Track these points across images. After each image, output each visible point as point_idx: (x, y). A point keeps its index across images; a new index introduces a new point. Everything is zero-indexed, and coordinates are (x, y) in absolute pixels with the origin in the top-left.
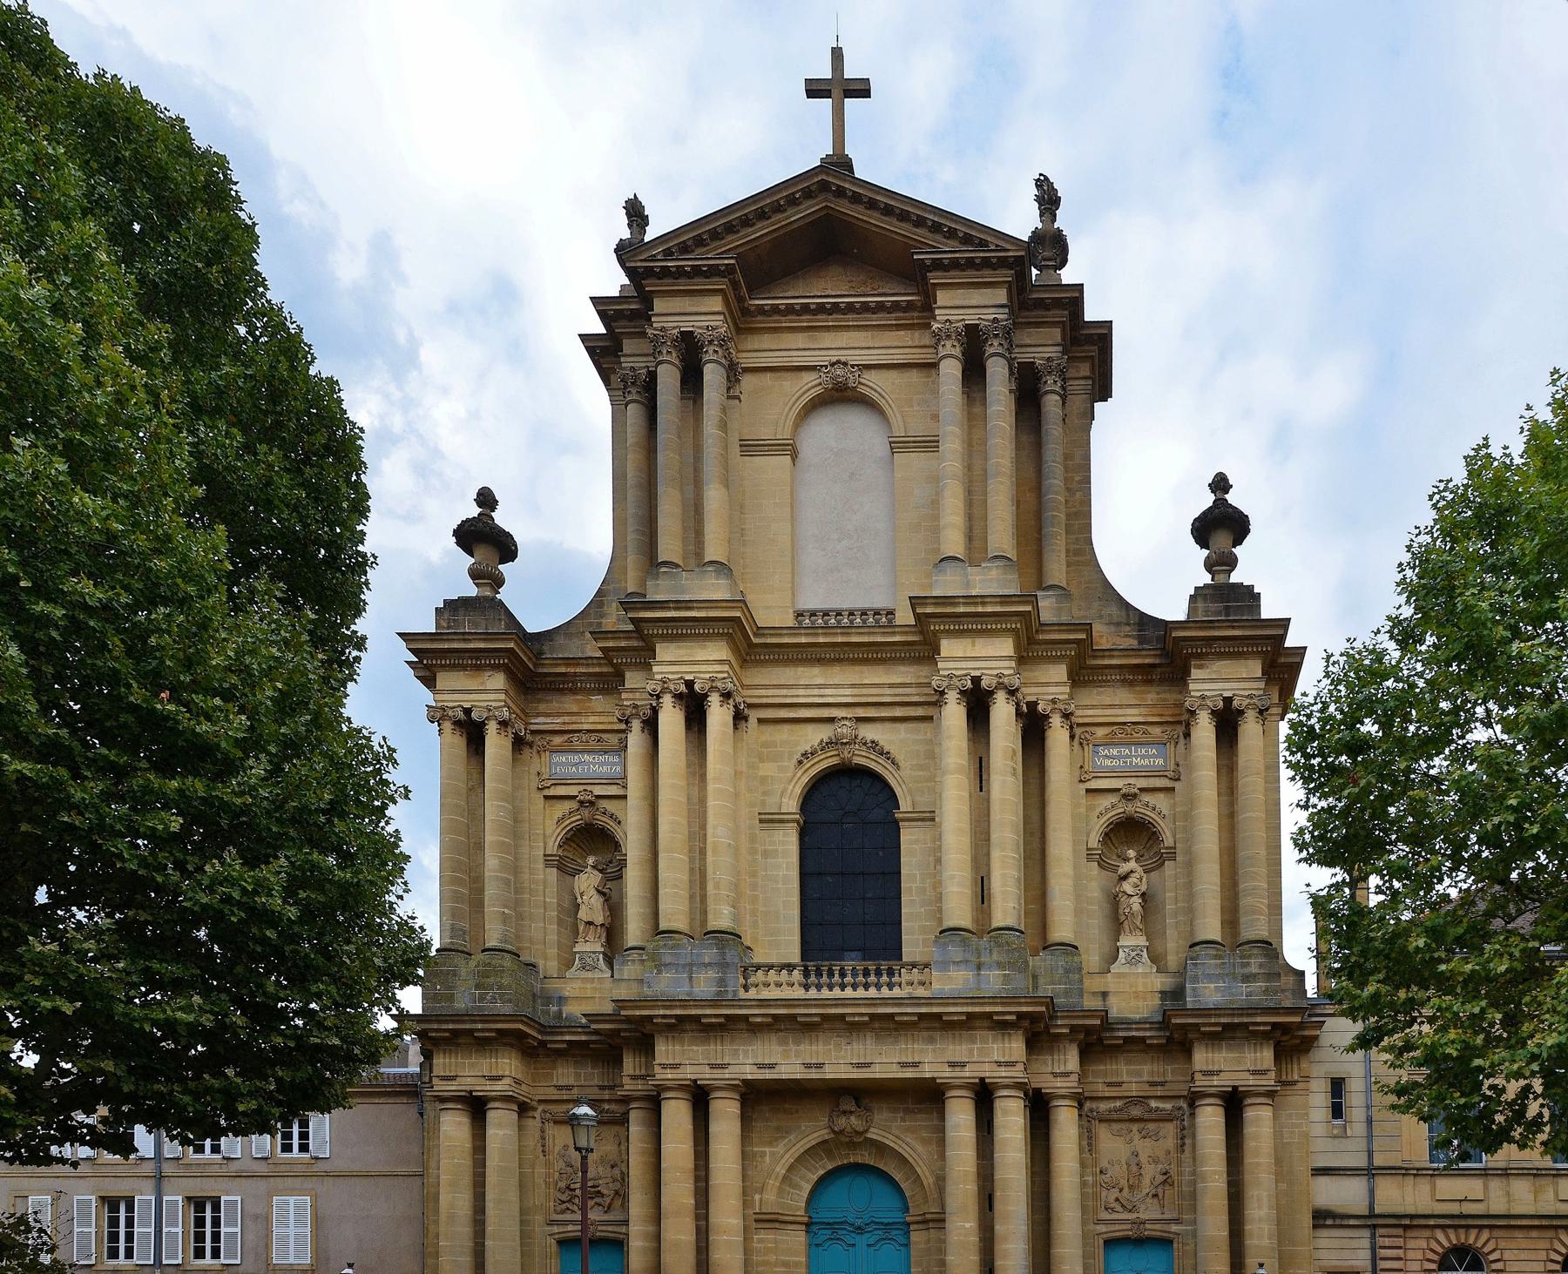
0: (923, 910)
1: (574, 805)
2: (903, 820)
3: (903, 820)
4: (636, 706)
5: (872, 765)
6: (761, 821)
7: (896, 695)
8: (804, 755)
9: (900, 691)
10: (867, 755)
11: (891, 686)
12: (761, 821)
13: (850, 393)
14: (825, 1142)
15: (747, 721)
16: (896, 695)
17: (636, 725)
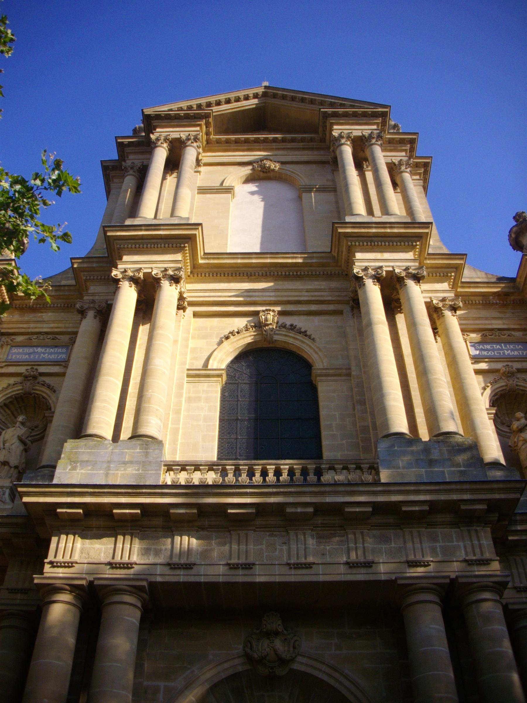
0: (344, 442)
1: (18, 379)
2: (320, 375)
3: (320, 375)
4: (93, 301)
5: (291, 341)
6: (188, 376)
7: (313, 296)
8: (232, 333)
9: (316, 294)
10: (287, 334)
11: (308, 291)
12: (188, 376)
13: (271, 174)
14: (235, 676)
15: (184, 312)
16: (313, 296)
17: (91, 314)
